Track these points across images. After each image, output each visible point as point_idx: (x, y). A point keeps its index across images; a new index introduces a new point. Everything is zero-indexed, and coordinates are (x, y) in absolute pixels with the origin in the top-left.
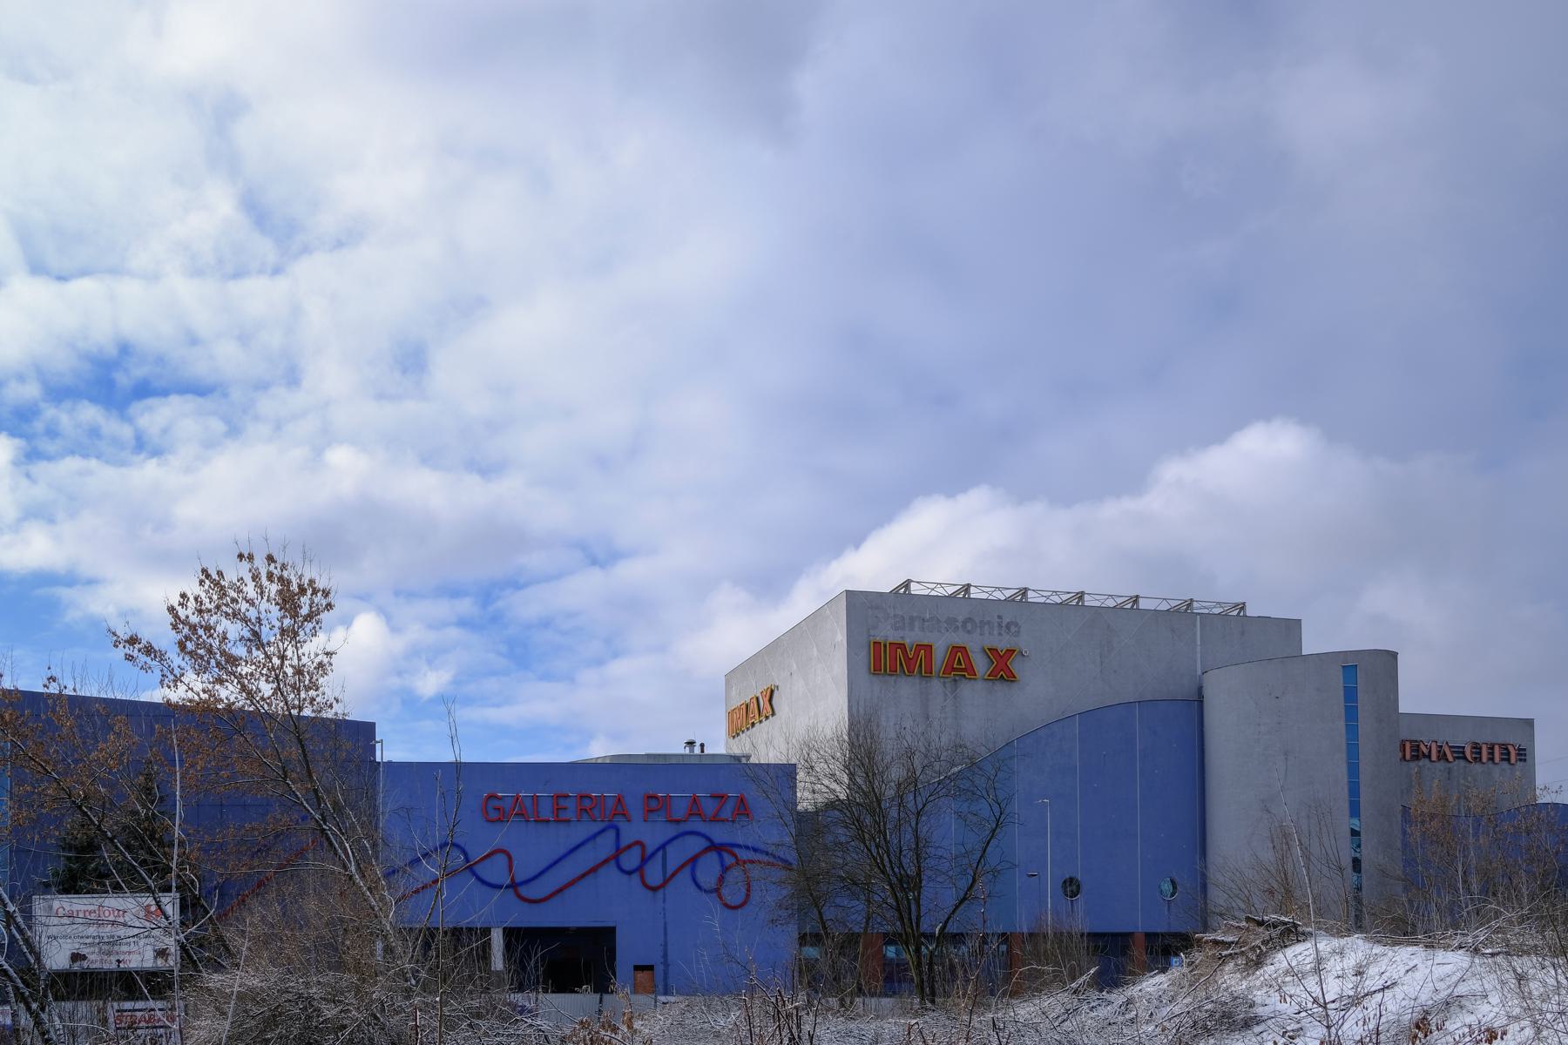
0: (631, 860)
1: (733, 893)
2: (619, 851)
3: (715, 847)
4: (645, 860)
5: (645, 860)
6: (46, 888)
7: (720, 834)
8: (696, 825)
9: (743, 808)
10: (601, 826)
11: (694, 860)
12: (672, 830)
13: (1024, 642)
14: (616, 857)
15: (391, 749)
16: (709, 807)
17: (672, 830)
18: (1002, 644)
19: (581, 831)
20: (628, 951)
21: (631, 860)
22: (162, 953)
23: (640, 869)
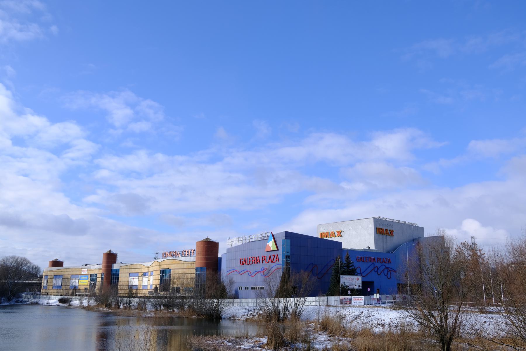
0: (376, 269)
1: (389, 276)
2: (374, 268)
3: (387, 268)
6: (343, 274)
7: (387, 265)
8: (384, 264)
9: (390, 261)
10: (371, 263)
12: (381, 264)
13: (394, 229)
14: (374, 269)
15: (344, 246)
16: (385, 260)
17: (381, 264)
18: (391, 229)
19: (370, 263)
20: (376, 286)
21: (376, 269)
22: (359, 286)
23: (377, 271)
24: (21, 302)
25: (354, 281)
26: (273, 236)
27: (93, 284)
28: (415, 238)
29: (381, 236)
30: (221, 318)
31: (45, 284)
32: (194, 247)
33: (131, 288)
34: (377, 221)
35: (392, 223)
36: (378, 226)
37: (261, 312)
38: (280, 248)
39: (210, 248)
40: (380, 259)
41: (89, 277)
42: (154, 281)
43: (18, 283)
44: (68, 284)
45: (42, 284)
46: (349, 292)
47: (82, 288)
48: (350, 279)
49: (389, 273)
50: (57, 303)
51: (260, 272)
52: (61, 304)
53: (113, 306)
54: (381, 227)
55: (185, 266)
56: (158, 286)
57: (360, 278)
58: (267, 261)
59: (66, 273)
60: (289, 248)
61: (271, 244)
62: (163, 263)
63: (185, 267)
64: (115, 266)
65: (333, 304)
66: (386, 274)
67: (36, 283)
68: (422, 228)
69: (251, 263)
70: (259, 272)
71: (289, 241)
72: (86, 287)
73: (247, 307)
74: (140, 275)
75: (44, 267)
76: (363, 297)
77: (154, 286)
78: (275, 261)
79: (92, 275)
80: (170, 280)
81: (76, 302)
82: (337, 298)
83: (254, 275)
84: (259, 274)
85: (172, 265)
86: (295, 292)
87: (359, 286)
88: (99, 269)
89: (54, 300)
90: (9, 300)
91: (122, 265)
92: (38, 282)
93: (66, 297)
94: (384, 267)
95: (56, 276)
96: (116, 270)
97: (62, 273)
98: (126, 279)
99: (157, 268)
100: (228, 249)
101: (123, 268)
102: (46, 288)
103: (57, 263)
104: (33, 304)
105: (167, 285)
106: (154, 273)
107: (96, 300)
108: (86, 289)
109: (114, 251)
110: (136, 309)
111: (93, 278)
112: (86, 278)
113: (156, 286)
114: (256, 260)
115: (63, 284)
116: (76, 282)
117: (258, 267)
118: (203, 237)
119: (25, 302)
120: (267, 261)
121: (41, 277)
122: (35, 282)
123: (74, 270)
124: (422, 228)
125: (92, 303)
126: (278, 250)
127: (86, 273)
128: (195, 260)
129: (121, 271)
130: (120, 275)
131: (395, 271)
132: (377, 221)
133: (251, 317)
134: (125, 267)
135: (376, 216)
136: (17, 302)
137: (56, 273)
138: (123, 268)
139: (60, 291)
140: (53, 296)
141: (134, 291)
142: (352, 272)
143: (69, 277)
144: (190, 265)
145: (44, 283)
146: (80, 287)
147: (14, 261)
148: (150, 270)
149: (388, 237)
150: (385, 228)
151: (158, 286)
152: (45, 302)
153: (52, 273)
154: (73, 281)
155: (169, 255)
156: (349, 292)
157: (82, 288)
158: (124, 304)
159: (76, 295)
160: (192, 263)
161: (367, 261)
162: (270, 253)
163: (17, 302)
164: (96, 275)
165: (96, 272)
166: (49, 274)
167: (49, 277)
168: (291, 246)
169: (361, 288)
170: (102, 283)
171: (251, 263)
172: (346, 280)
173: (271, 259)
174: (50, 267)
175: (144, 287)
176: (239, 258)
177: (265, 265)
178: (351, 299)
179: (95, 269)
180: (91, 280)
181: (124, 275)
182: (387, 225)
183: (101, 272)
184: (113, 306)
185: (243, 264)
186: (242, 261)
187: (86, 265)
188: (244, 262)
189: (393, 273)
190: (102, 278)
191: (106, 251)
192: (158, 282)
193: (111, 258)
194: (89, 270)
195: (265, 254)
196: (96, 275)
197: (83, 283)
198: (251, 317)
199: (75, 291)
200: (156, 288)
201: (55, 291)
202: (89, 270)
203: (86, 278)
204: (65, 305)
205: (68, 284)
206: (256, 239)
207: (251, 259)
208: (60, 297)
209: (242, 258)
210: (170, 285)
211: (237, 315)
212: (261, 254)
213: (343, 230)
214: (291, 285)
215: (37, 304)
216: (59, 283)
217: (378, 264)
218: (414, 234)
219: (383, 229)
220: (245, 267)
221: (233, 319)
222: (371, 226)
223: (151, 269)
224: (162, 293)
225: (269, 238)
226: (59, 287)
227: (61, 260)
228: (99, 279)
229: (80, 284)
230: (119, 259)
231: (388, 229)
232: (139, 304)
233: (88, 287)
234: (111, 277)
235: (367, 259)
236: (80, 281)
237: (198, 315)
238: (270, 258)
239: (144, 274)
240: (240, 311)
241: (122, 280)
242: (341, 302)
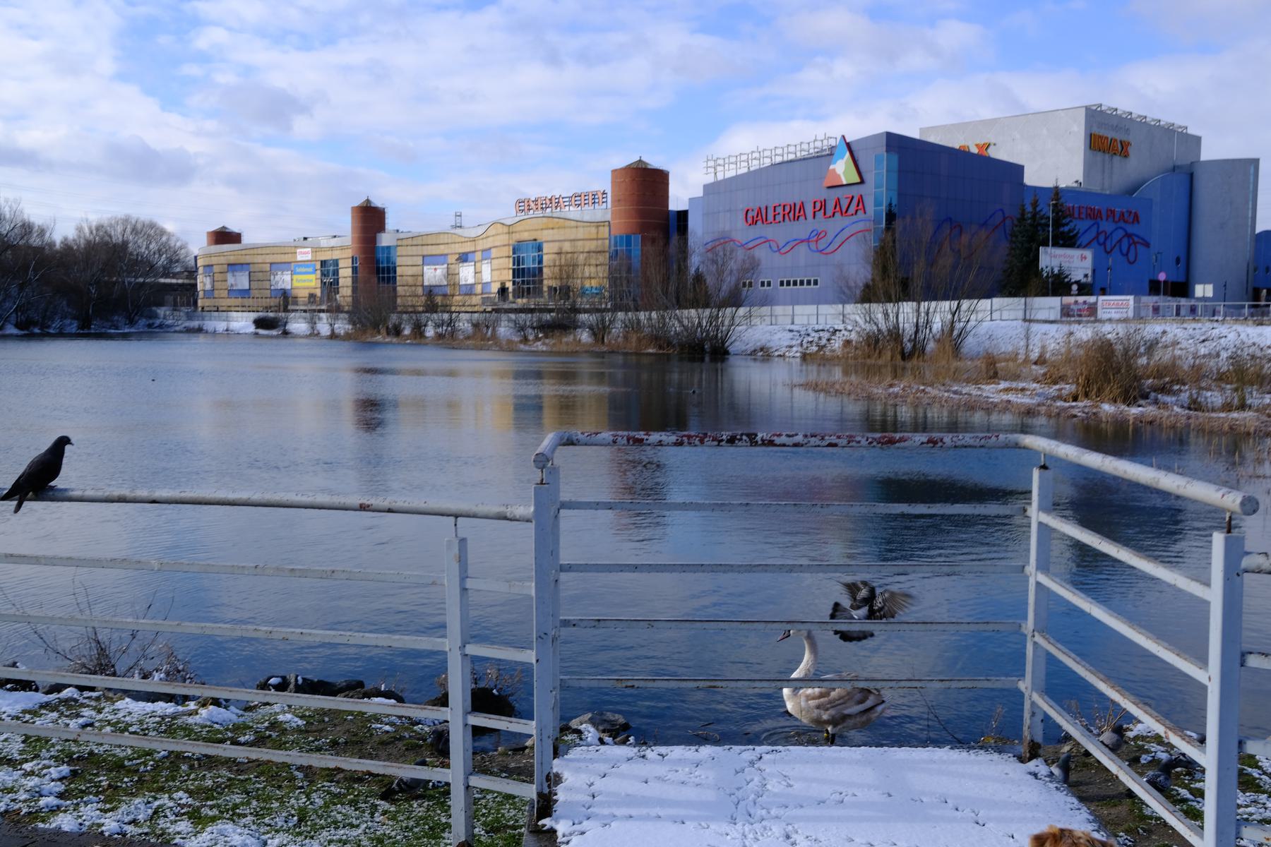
0: (1102, 238)
1: (1131, 258)
2: (1098, 234)
3: (1128, 235)
4: (1106, 239)
5: (1106, 239)
7: (1131, 229)
8: (1122, 224)
9: (1136, 218)
11: (1120, 241)
13: (1131, 138)
14: (1097, 237)
15: (1030, 179)
18: (1124, 138)
21: (1102, 238)
23: (1104, 243)
24: (160, 326)
25: (1077, 262)
26: (848, 145)
27: (330, 286)
28: (1179, 163)
29: (1099, 155)
30: (727, 352)
31: (208, 287)
32: (604, 184)
33: (430, 292)
34: (1094, 115)
35: (1124, 122)
36: (1096, 130)
37: (853, 336)
38: (870, 178)
39: (646, 184)
40: (1113, 212)
41: (318, 266)
42: (496, 273)
43: (143, 284)
44: (266, 284)
45: (199, 287)
46: (1075, 287)
47: (303, 294)
48: (1065, 256)
49: (1133, 247)
50: (252, 329)
51: (808, 240)
52: (261, 332)
53: (407, 332)
54: (1102, 132)
55: (581, 233)
56: (509, 285)
57: (1088, 254)
58: (829, 213)
59: (259, 259)
60: (895, 176)
61: (842, 169)
62: (518, 228)
63: (580, 236)
64: (385, 240)
65: (1041, 315)
66: (1125, 251)
67: (182, 285)
68: (1198, 140)
69: (779, 218)
70: (802, 241)
71: (895, 158)
72: (313, 291)
73: (792, 327)
74: (452, 259)
75: (196, 245)
76: (1131, 298)
77: (495, 288)
78: (852, 209)
79: (323, 263)
80: (540, 270)
81: (298, 325)
82: (1055, 302)
83: (787, 248)
84: (803, 248)
85: (545, 232)
86: (904, 292)
87: (1086, 276)
88: (342, 248)
89: (243, 322)
90: (132, 322)
91: (402, 236)
92: (186, 281)
93: (271, 315)
94: (1120, 233)
95: (233, 267)
96: (388, 248)
97: (248, 259)
98: (410, 271)
99: (503, 239)
100: (706, 187)
101: (404, 242)
102: (210, 294)
103: (224, 237)
104: (189, 331)
105: (534, 282)
106: (494, 253)
107: (352, 322)
108: (312, 296)
109: (377, 202)
110: (468, 338)
111: (328, 269)
112: (311, 270)
113: (503, 284)
114: (794, 212)
115: (254, 285)
116: (284, 280)
117: (801, 229)
118: (631, 159)
119: (168, 326)
120: (829, 213)
121: (192, 273)
122: (180, 281)
123: (276, 250)
124: (1198, 140)
125: (342, 326)
126: (862, 182)
127: (309, 257)
128: (608, 217)
129: (400, 251)
130: (399, 261)
131: (1147, 245)
132: (1094, 115)
133: (815, 349)
134: (410, 242)
135: (1092, 100)
136: (150, 326)
137: (232, 259)
138: (404, 242)
139: (247, 302)
140: (234, 314)
141: (439, 299)
142: (1067, 241)
143: (267, 267)
144: (593, 230)
145: (203, 282)
146: (294, 293)
147: (129, 230)
148: (480, 247)
149: (1117, 159)
150: (1110, 134)
151: (509, 285)
152: (221, 326)
153: (222, 260)
154: (277, 278)
155: (532, 205)
156: (1075, 287)
157: (303, 294)
158: (437, 326)
159: (293, 311)
160: (598, 224)
161: (1083, 216)
162: (838, 193)
163: (150, 326)
164: (336, 262)
165: (336, 255)
166: (214, 260)
167: (216, 269)
168: (900, 171)
169: (1090, 279)
170: (355, 280)
171: (779, 218)
172: (1051, 259)
173: (841, 203)
174: (210, 244)
175: (469, 290)
176: (742, 206)
177: (820, 223)
178: (1096, 303)
179: (332, 248)
180: (323, 274)
181: (409, 261)
182: (1116, 128)
183: (349, 253)
184: (407, 332)
185: (754, 222)
186: (750, 214)
187: (305, 239)
188: (756, 217)
189: (1139, 247)
190: (355, 270)
191: (358, 202)
192: (508, 275)
193: (370, 218)
194: (316, 250)
195: (823, 195)
196: (336, 262)
197: (306, 283)
198: (815, 349)
199: (286, 300)
200: (503, 290)
201: (239, 301)
202: (316, 250)
203: (311, 270)
204: (274, 332)
205: (266, 284)
206: (792, 157)
207: (780, 210)
208: (254, 316)
209: (751, 206)
210: (541, 282)
211: (771, 344)
212: (808, 194)
213: (993, 141)
214: (893, 277)
215: (200, 330)
216: (242, 281)
217: (1107, 226)
218: (1179, 156)
219: (1107, 137)
220: (761, 230)
221: (763, 354)
222: (1075, 128)
223: (481, 245)
224: (519, 301)
225: (837, 152)
226: (244, 293)
227: (234, 227)
228: (345, 273)
229: (296, 284)
230: (390, 223)
231: (1119, 136)
232: (476, 326)
233: (318, 292)
234: (375, 265)
235: (1083, 211)
236: (295, 277)
237: (660, 347)
238: (838, 202)
239: (463, 258)
240: (776, 337)
241: (404, 270)
242: (1066, 312)
